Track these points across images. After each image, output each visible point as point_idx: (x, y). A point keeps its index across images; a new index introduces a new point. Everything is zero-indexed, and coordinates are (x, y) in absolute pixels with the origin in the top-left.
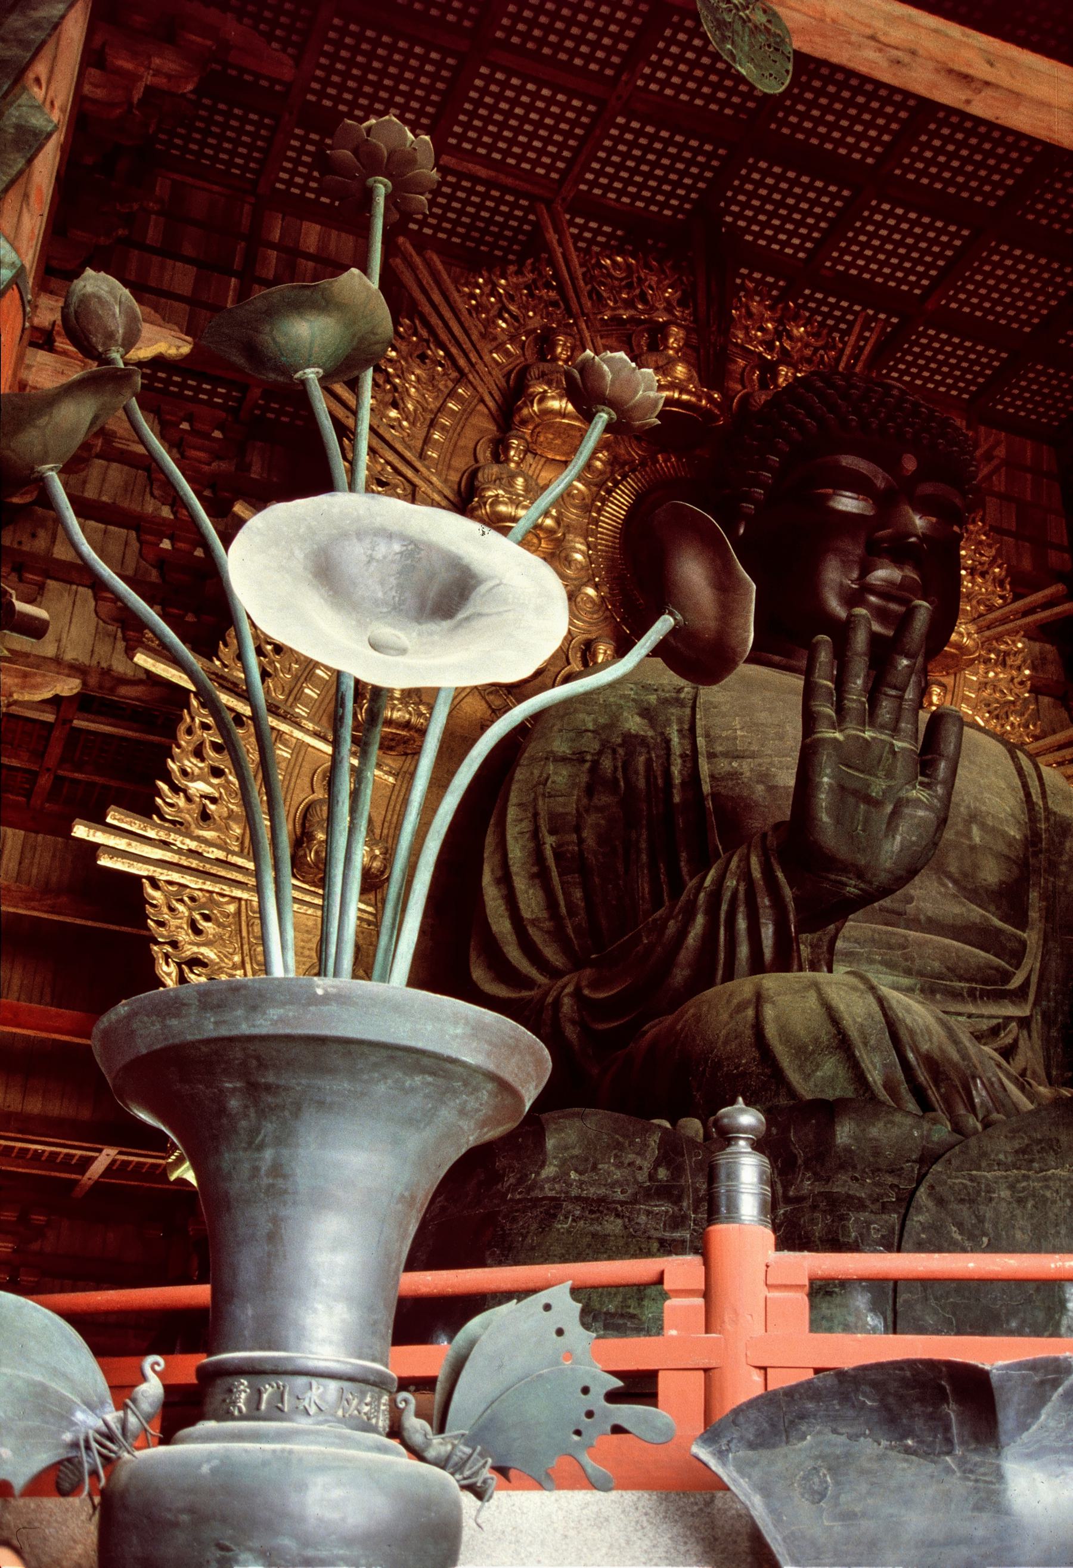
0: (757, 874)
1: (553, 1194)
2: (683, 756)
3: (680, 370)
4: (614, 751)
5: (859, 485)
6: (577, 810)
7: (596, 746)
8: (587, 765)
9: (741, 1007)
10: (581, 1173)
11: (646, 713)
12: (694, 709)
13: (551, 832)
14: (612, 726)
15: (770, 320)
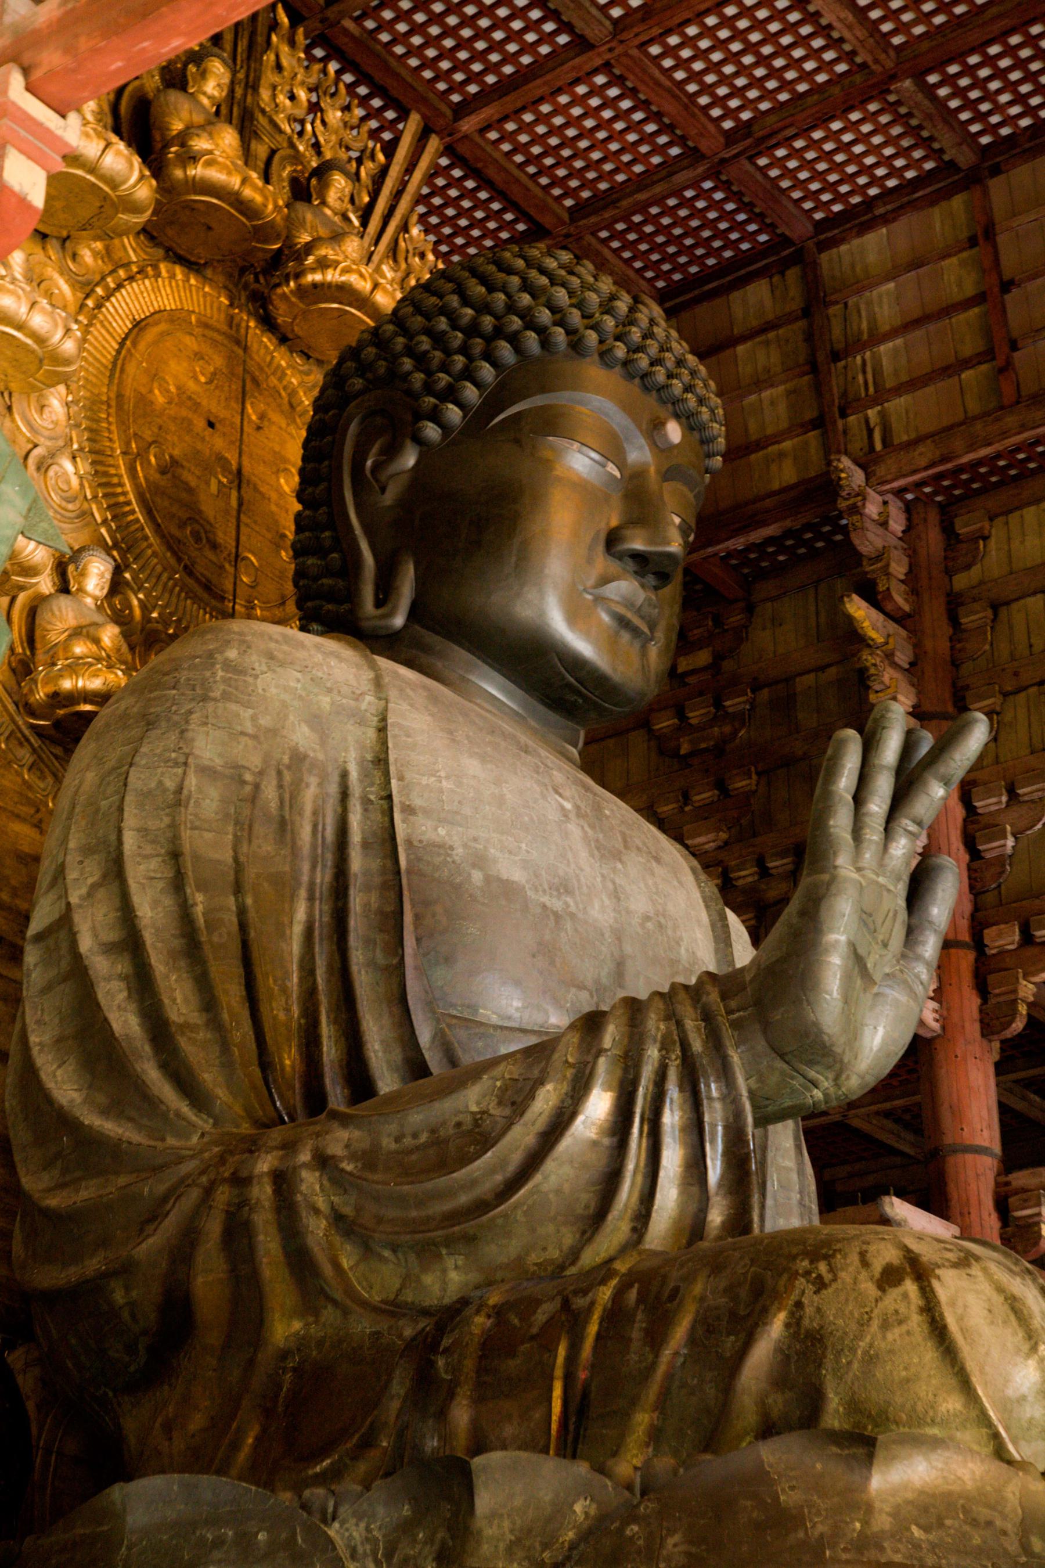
0: (697, 1045)
1: (898, 1558)
2: (366, 802)
3: (228, 138)
4: (279, 773)
5: (612, 449)
6: (236, 859)
7: (255, 761)
8: (248, 789)
9: (889, 1278)
10: (927, 1529)
11: (316, 721)
12: (382, 730)
13: (199, 890)
14: (273, 732)
15: (303, 83)
